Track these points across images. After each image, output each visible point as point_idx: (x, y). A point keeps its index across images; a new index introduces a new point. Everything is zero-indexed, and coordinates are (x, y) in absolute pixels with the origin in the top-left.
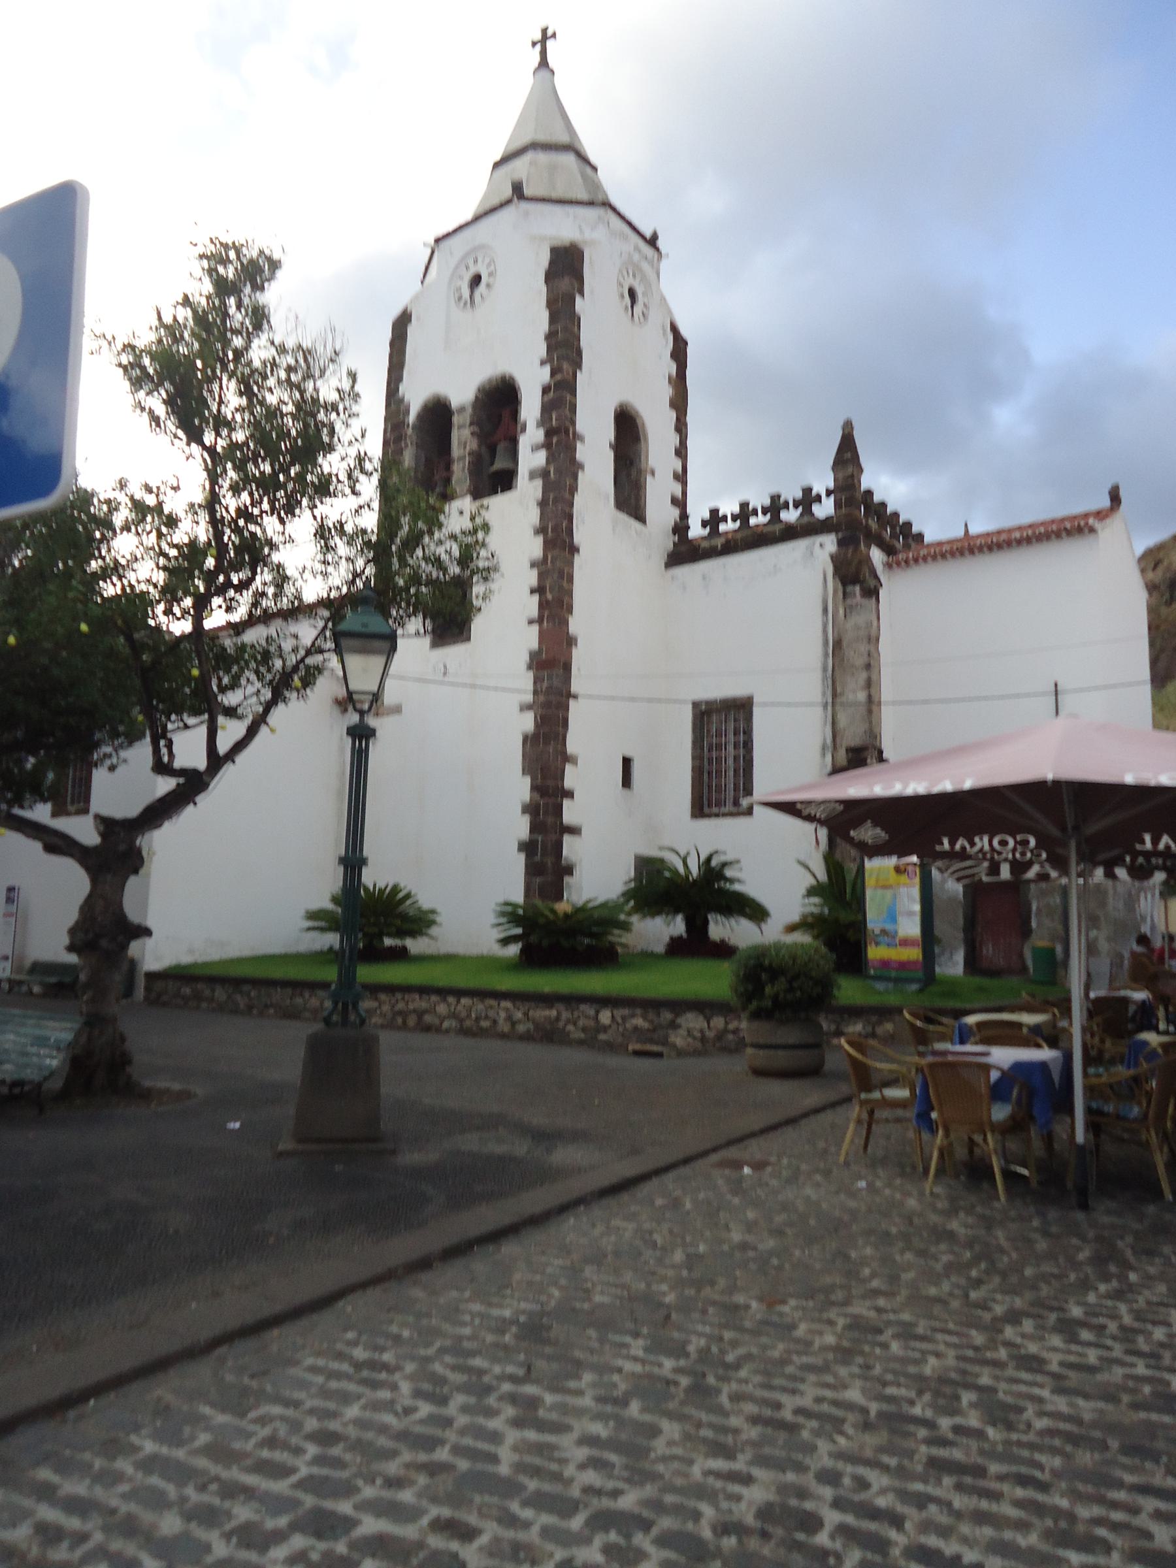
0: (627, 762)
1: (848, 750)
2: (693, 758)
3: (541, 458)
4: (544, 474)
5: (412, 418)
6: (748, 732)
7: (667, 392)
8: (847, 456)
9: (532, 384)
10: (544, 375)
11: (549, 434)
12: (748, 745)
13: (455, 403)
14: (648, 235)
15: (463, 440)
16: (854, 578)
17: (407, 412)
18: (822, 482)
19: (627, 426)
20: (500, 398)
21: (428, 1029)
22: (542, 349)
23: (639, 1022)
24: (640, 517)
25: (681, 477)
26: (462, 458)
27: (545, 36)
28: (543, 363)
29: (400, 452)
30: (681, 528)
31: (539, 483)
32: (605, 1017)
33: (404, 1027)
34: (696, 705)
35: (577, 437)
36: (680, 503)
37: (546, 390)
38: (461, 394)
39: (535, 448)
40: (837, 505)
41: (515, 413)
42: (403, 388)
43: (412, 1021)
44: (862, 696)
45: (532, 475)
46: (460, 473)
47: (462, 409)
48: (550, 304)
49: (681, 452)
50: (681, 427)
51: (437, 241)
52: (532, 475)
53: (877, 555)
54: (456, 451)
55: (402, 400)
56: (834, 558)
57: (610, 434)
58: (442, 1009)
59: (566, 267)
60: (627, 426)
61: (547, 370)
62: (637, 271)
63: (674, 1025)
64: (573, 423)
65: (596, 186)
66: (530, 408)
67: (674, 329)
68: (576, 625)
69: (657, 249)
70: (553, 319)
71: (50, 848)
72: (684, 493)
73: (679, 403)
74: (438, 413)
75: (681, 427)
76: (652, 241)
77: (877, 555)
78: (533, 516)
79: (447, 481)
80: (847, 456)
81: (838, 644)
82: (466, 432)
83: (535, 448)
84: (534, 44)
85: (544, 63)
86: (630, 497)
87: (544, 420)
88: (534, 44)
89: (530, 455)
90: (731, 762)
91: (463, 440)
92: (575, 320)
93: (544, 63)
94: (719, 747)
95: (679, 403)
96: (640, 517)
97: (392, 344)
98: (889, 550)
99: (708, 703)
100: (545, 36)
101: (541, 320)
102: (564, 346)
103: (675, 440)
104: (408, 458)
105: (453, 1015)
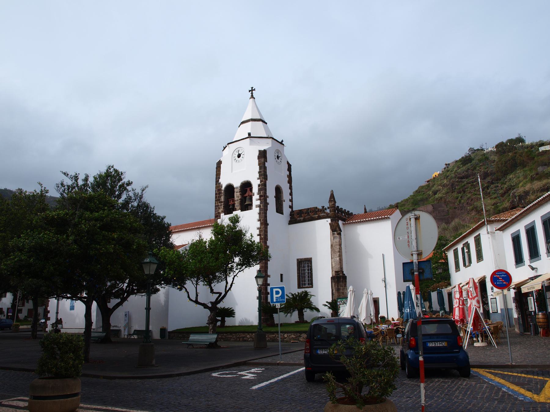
0: (281, 275)
1: (335, 272)
2: (298, 273)
3: (258, 202)
4: (259, 206)
5: (223, 188)
6: (311, 267)
7: (287, 179)
8: (332, 198)
9: (256, 184)
10: (259, 182)
11: (260, 196)
12: (311, 269)
13: (235, 186)
14: (280, 141)
15: (237, 195)
16: (335, 229)
17: (222, 187)
18: (327, 205)
19: (278, 190)
20: (246, 186)
21: (245, 341)
22: (257, 175)
23: (293, 336)
24: (282, 214)
25: (291, 200)
26: (237, 200)
27: (252, 90)
28: (258, 179)
29: (220, 197)
30: (292, 214)
31: (258, 208)
32: (286, 336)
33: (239, 341)
34: (298, 260)
35: (267, 197)
36: (291, 207)
37: (259, 185)
38: (237, 184)
39: (257, 200)
40: (330, 211)
41: (251, 190)
42: (220, 181)
43: (241, 339)
44: (338, 259)
45: (257, 206)
46: (237, 204)
47: (237, 188)
48: (259, 165)
49: (291, 194)
50: (291, 188)
51: (228, 144)
52: (257, 206)
53: (340, 223)
54: (236, 198)
55: (220, 183)
56: (330, 224)
57: (274, 194)
58: (248, 336)
59: (263, 155)
60: (278, 190)
61: (259, 180)
62: (278, 151)
63: (300, 336)
64: (266, 193)
65: (267, 130)
66: (255, 190)
67: (288, 163)
68: (268, 243)
69: (283, 144)
70: (260, 168)
71: (205, 308)
72: (292, 204)
73: (290, 182)
74: (230, 188)
75: (291, 188)
76: (281, 143)
77: (340, 223)
78: (257, 217)
79: (234, 205)
80: (332, 198)
81: (332, 246)
82: (238, 194)
83: (257, 200)
84: (250, 91)
85: (252, 97)
86: (279, 210)
87: (259, 194)
88: (250, 91)
89: (256, 201)
90: (307, 274)
91: (237, 195)
92: (265, 168)
93: (252, 97)
94: (304, 270)
95: (290, 182)
96: (282, 214)
97: (217, 168)
98: (343, 220)
99: (301, 259)
100: (252, 90)
101: (257, 168)
102: (263, 175)
103: (290, 191)
104: (222, 199)
105: (251, 337)
